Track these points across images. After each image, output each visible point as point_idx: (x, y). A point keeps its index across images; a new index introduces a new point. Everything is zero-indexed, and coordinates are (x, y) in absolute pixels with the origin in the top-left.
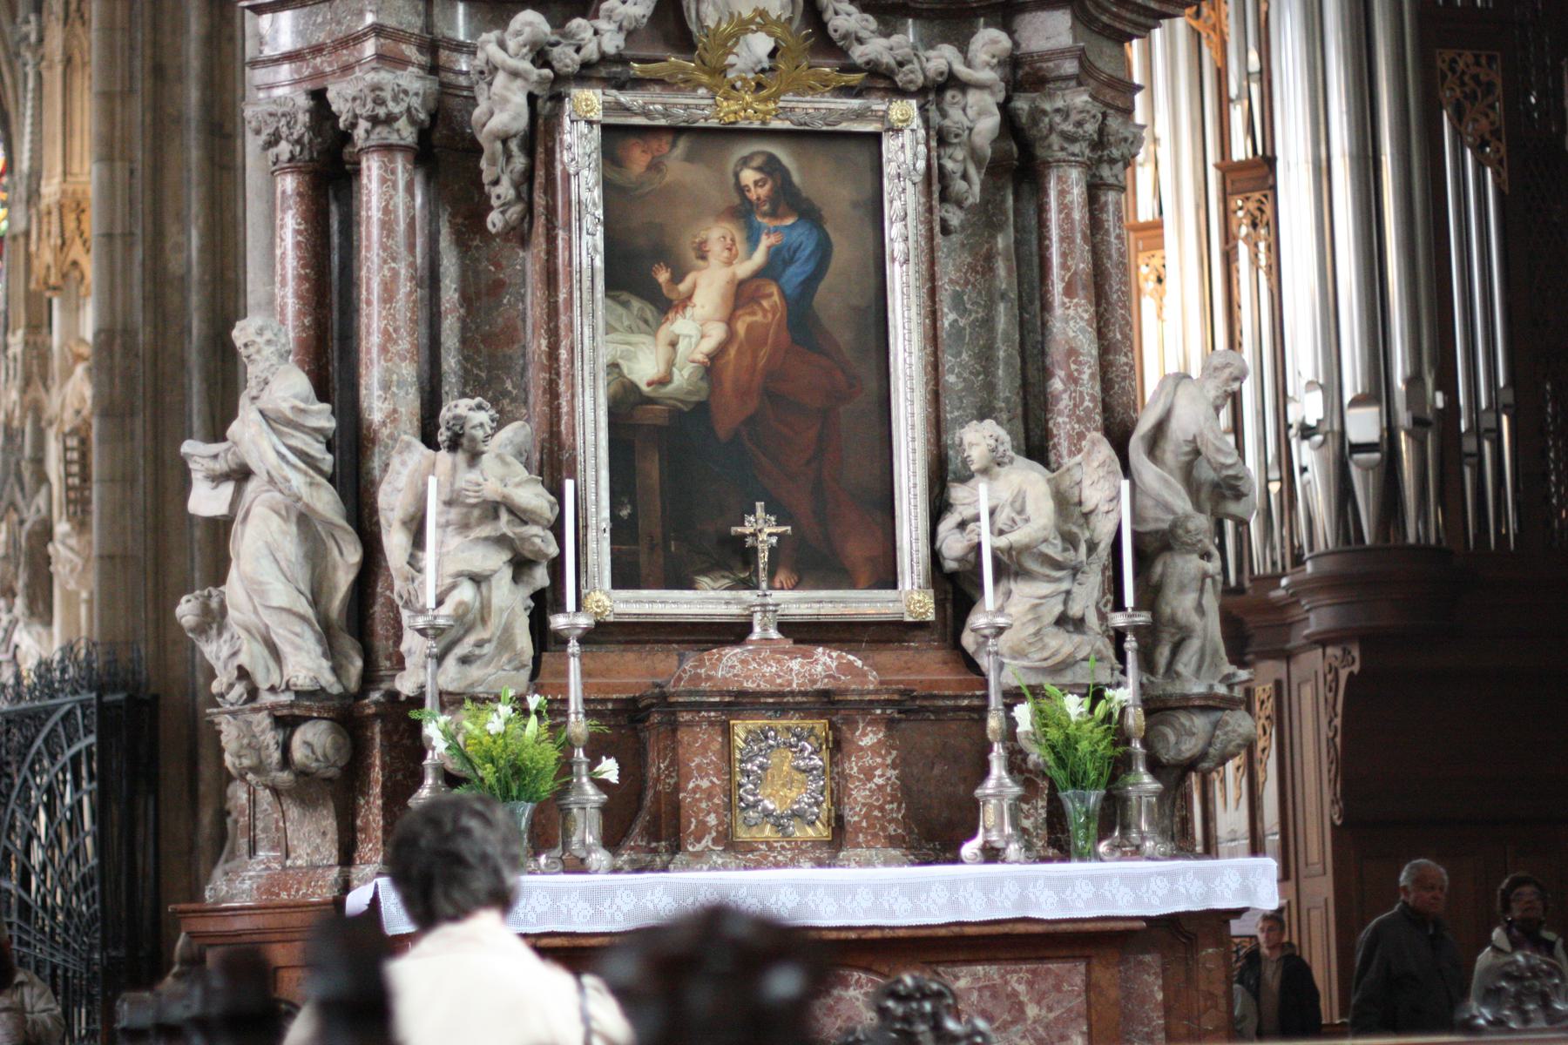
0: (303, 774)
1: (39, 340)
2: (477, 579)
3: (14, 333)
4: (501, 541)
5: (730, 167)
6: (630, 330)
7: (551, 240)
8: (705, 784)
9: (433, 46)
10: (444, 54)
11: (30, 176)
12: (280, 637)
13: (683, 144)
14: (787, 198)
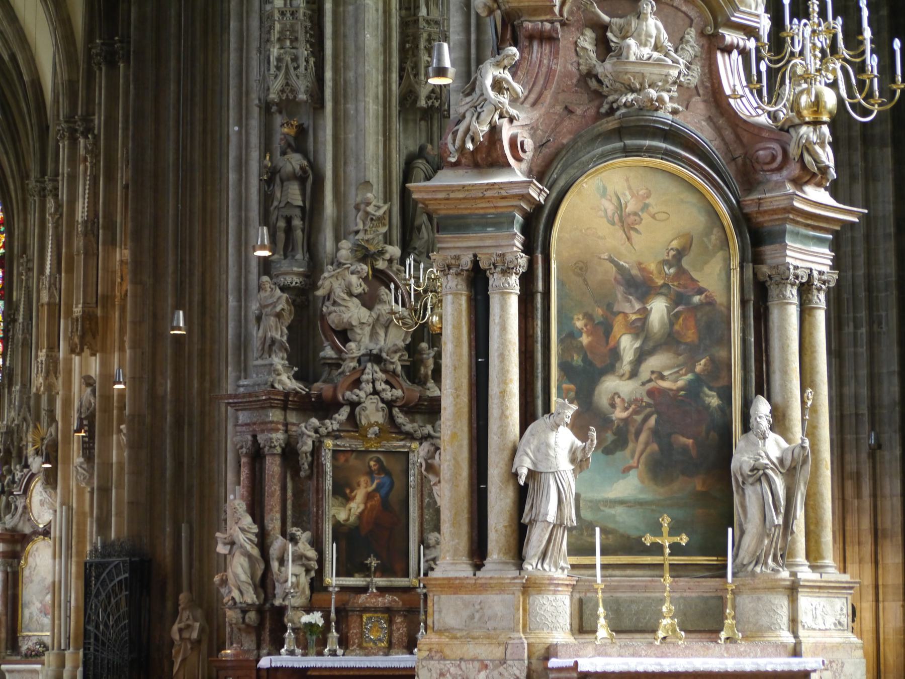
0: (248, 626)
1: (53, 354)
2: (296, 576)
3: (41, 351)
4: (303, 565)
5: (367, 461)
6: (339, 506)
7: (318, 481)
8: (355, 631)
9: (286, 425)
10: (289, 427)
11: (50, 276)
12: (243, 588)
13: (354, 455)
14: (382, 469)
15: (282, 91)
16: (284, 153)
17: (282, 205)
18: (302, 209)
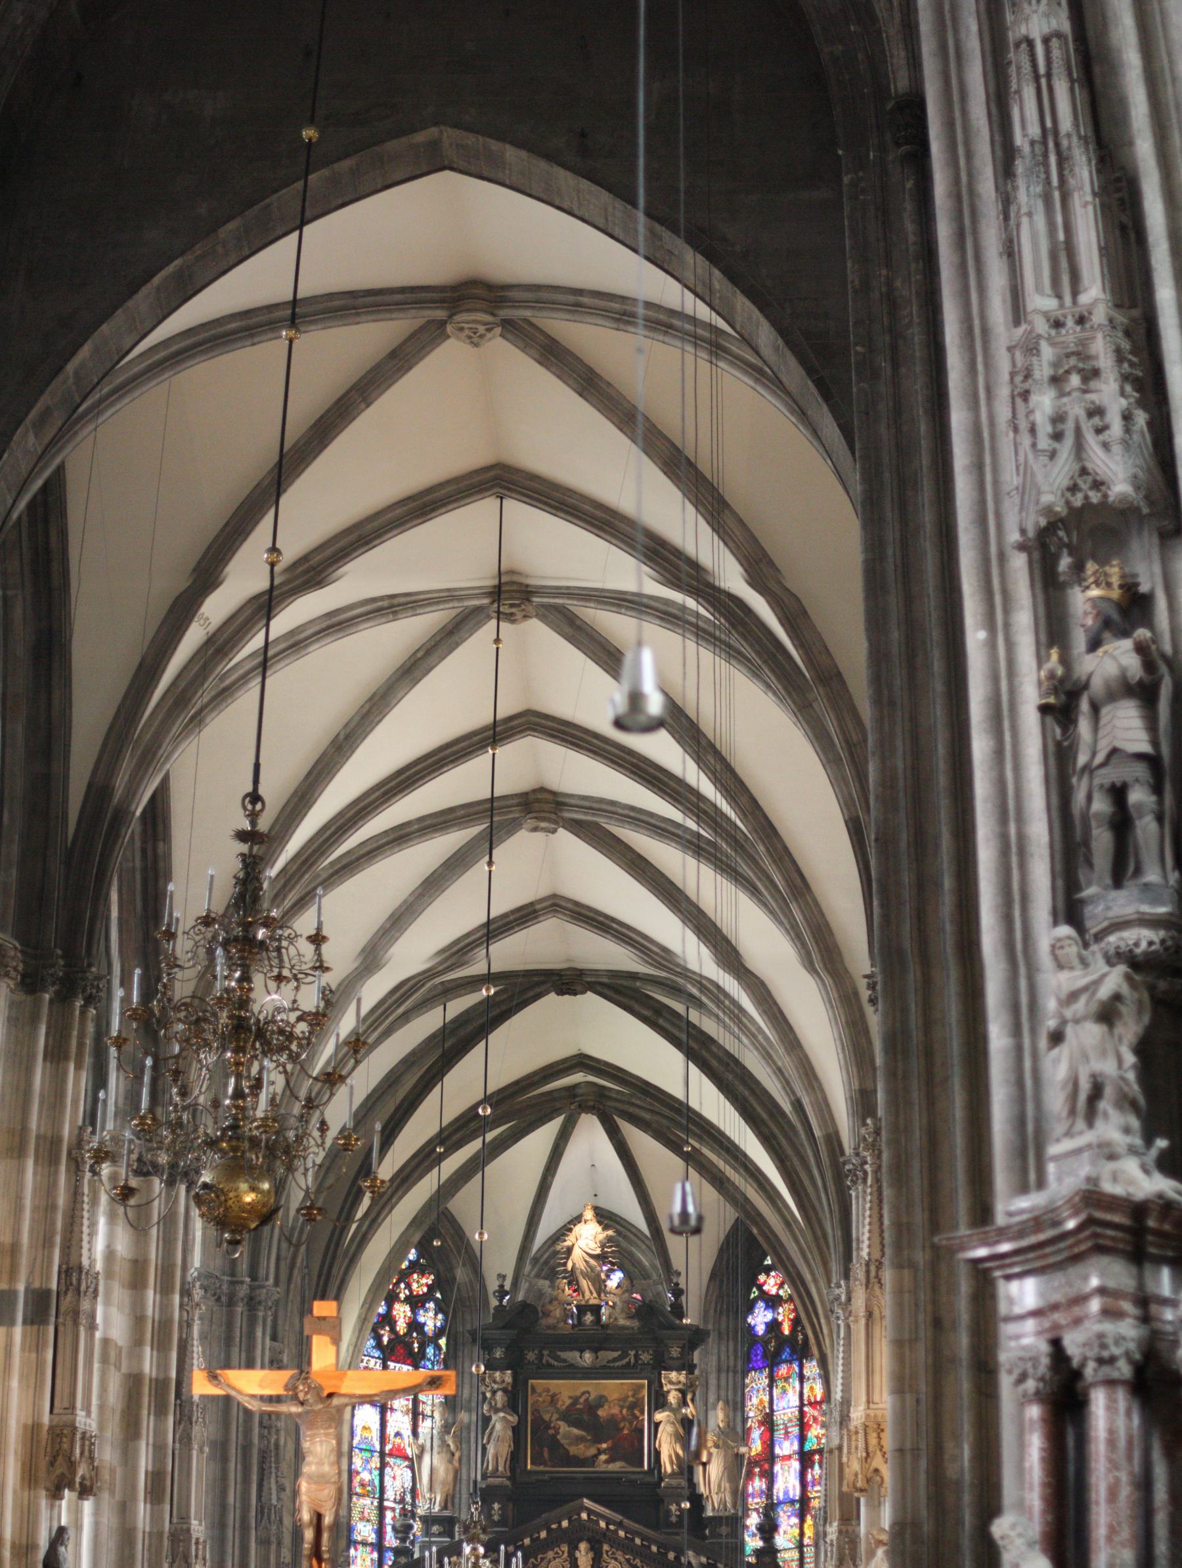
1: (850, 1529)
3: (831, 1525)
9: (1145, 1302)
10: (1154, 1308)
11: (842, 1404)
15: (1073, 488)
16: (1094, 644)
17: (1100, 758)
18: (1152, 761)
